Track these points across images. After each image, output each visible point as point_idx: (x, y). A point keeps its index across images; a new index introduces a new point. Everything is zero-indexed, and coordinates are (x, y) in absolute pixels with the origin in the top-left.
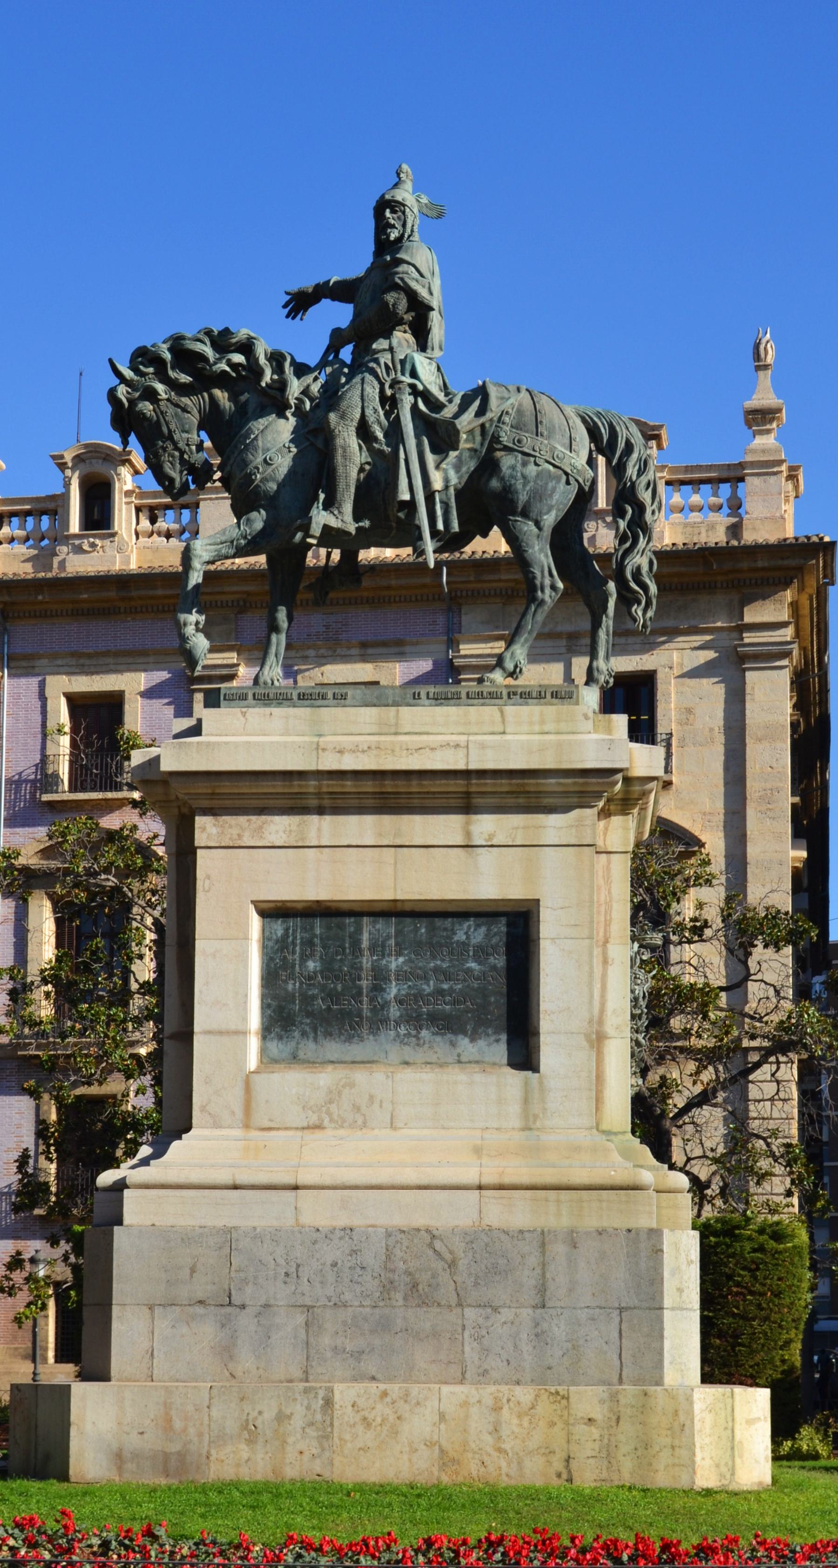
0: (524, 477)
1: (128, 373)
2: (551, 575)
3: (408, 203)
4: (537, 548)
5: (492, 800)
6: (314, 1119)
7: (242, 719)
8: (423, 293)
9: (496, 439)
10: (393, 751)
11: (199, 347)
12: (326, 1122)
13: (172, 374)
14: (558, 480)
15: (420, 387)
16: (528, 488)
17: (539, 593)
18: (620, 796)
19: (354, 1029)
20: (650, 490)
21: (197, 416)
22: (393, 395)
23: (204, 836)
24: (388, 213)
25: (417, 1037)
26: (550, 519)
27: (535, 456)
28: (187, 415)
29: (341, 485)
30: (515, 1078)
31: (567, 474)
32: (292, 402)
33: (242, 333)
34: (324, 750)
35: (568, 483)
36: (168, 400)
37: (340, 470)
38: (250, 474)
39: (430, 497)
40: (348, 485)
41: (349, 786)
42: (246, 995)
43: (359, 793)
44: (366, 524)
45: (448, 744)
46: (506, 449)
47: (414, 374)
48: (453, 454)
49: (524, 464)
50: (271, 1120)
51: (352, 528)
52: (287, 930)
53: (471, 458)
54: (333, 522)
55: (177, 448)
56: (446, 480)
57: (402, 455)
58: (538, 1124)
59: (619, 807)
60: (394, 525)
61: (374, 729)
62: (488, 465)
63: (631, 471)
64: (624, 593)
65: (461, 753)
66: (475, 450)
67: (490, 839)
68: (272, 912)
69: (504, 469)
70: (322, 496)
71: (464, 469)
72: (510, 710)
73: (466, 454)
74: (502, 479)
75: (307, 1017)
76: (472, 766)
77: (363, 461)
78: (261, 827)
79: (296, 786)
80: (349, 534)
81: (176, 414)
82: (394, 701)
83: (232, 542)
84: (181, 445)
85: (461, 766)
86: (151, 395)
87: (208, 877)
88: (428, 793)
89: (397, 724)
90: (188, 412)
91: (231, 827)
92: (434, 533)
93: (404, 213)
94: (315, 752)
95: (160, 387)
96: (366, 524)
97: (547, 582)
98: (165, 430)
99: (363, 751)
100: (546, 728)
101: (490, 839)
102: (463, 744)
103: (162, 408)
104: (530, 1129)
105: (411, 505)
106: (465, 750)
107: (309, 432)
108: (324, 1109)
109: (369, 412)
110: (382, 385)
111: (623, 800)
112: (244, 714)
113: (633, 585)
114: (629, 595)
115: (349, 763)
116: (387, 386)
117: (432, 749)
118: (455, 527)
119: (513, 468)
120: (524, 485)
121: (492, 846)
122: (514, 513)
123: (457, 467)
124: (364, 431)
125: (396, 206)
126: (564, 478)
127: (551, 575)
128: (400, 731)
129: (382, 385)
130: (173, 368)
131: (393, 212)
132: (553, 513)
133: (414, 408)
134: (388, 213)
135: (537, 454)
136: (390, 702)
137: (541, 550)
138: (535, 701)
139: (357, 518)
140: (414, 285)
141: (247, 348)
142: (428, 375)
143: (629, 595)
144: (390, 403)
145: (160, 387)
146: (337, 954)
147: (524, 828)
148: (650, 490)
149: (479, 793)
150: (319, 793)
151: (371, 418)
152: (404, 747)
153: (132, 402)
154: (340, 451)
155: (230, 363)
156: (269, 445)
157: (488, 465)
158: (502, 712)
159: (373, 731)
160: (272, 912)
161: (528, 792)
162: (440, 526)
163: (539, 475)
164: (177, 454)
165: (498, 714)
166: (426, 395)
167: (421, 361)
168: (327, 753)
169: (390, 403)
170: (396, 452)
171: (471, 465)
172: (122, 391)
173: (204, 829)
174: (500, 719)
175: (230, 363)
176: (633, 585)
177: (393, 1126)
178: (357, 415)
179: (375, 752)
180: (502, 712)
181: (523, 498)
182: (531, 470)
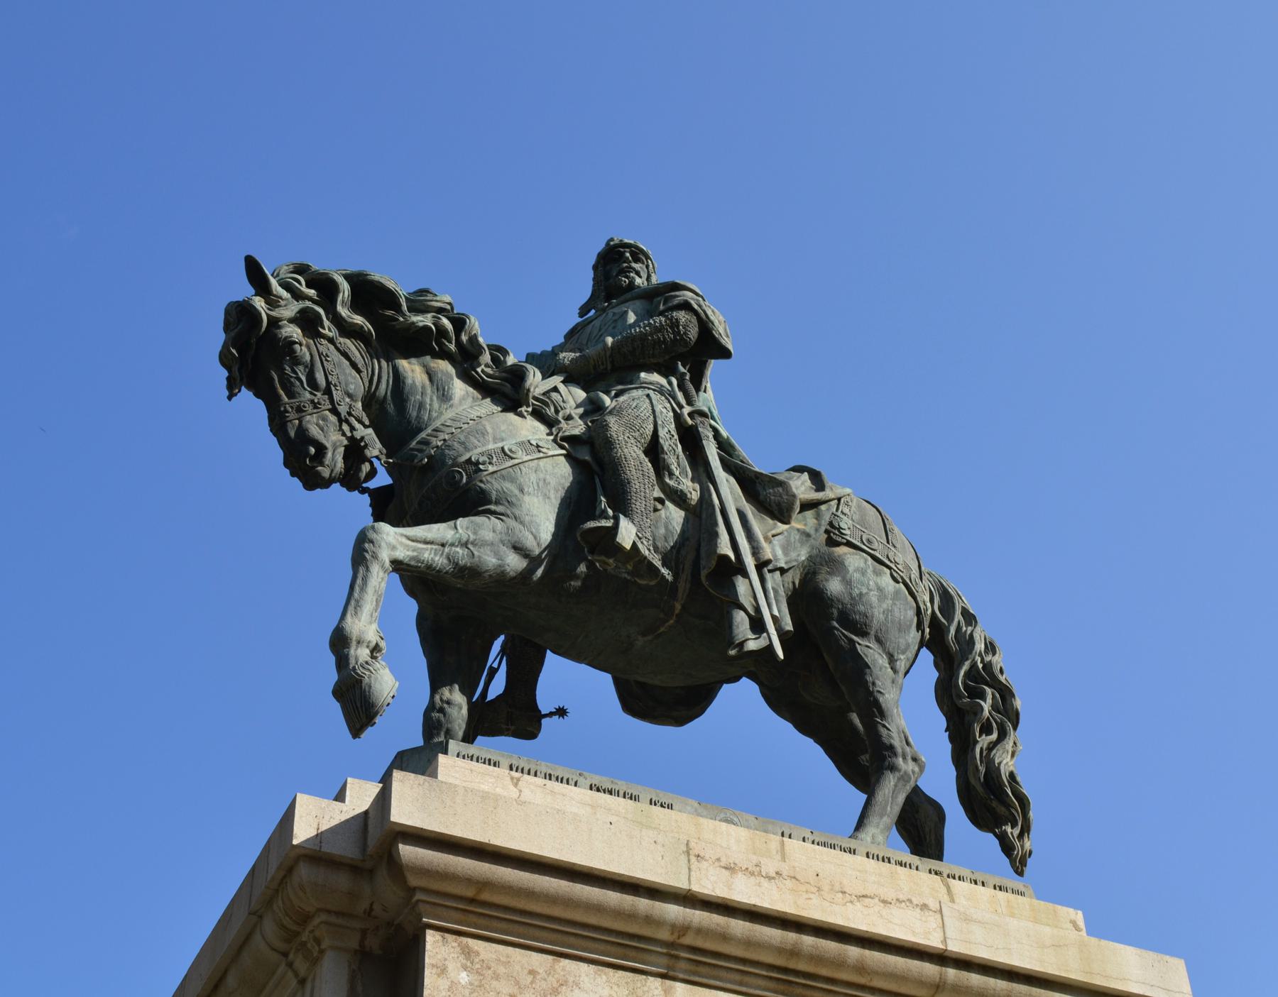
13: (344, 311)
16: (885, 606)
21: (367, 385)
27: (890, 568)
28: (354, 373)
38: (478, 463)
43: (744, 961)
45: (910, 901)
48: (782, 527)
55: (334, 411)
60: (678, 607)
64: (994, 804)
66: (808, 535)
69: (851, 569)
73: (796, 537)
74: (848, 583)
76: (956, 947)
81: (340, 365)
83: (443, 545)
90: (359, 371)
91: (497, 977)
94: (684, 858)
98: (320, 377)
99: (770, 878)
103: (321, 348)
109: (662, 433)
115: (744, 892)
117: (884, 902)
122: (864, 634)
135: (892, 565)
143: (1001, 810)
150: (671, 945)
152: (837, 888)
164: (333, 418)
168: (704, 864)
173: (443, 971)
179: (789, 883)
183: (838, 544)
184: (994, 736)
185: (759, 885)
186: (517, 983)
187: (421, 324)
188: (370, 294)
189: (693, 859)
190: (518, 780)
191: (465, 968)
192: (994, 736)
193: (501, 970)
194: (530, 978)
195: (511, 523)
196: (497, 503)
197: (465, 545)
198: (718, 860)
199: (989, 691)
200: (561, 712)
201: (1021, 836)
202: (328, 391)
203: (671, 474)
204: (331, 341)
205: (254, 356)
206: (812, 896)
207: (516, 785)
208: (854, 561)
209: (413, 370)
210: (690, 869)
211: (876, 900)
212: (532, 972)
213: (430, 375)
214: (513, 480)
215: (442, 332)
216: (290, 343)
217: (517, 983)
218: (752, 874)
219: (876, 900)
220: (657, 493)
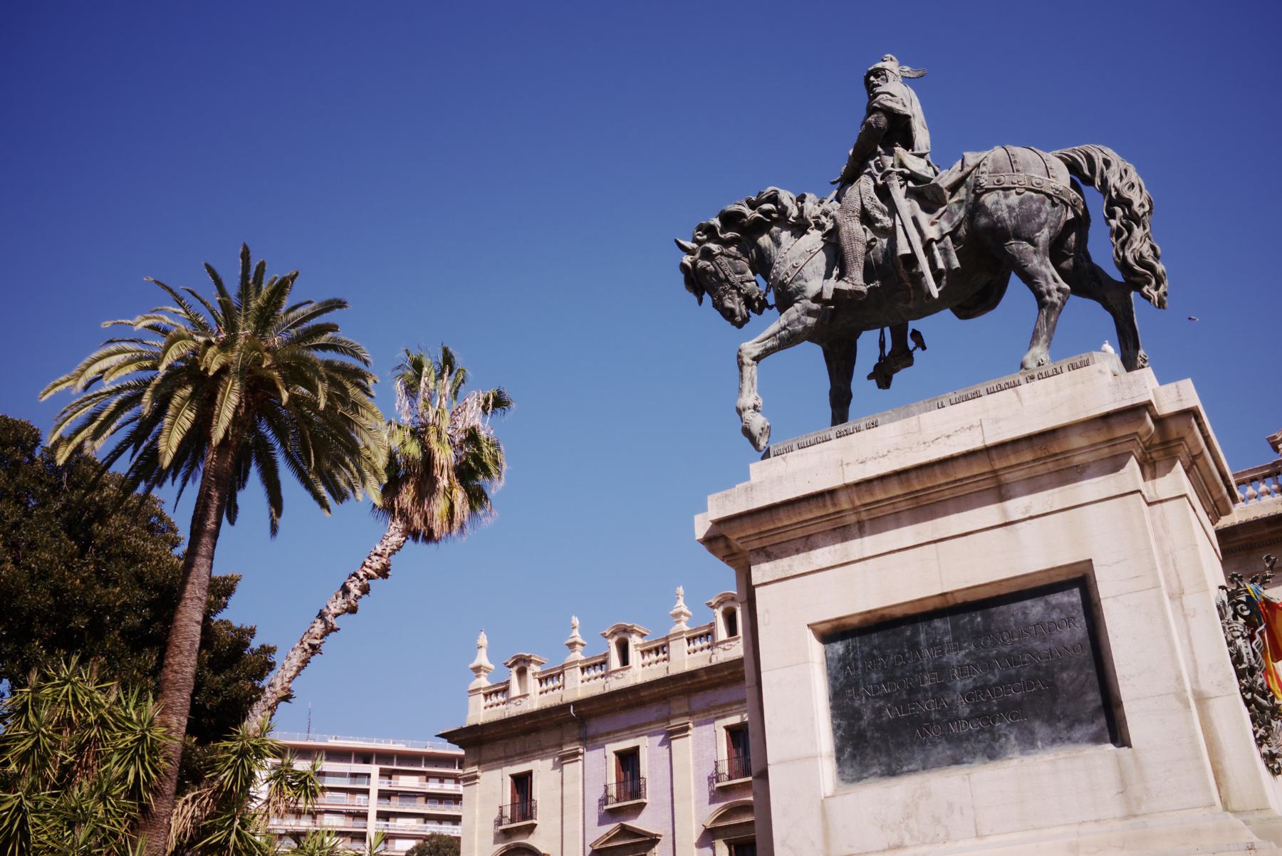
0: (1009, 207)
1: (689, 244)
2: (1056, 281)
4: (1036, 262)
5: (1022, 473)
6: (894, 839)
8: (898, 107)
9: (977, 185)
11: (734, 208)
12: (907, 841)
14: (1044, 203)
15: (907, 171)
17: (1047, 298)
19: (926, 735)
20: (1137, 188)
22: (885, 184)
23: (760, 573)
24: (872, 78)
25: (991, 732)
26: (1044, 236)
29: (850, 258)
30: (1101, 757)
31: (1049, 196)
32: (811, 221)
33: (769, 189)
35: (1054, 205)
36: (721, 254)
37: (847, 248)
40: (855, 258)
42: (813, 718)
44: (878, 283)
46: (988, 190)
47: (902, 165)
49: (1006, 197)
50: (851, 846)
51: (864, 289)
52: (847, 647)
53: (960, 208)
54: (843, 285)
57: (898, 222)
58: (1144, 809)
59: (1161, 453)
62: (976, 208)
63: (1113, 180)
67: (1027, 511)
68: (831, 634)
70: (835, 272)
72: (1025, 388)
75: (877, 731)
80: (861, 293)
84: (737, 283)
85: (978, 444)
86: (708, 255)
87: (767, 611)
88: (955, 481)
92: (937, 275)
95: (714, 247)
96: (878, 283)
97: (1053, 286)
98: (722, 276)
101: (1027, 511)
102: (976, 423)
104: (1136, 816)
105: (911, 259)
108: (903, 826)
110: (875, 180)
111: (1162, 444)
112: (784, 459)
113: (1137, 268)
114: (1138, 279)
116: (878, 179)
118: (956, 263)
119: (997, 203)
120: (1010, 213)
121: (1031, 518)
123: (950, 220)
124: (866, 218)
125: (878, 73)
126: (1048, 201)
127: (1056, 281)
129: (875, 180)
130: (722, 232)
131: (877, 76)
132: (1046, 231)
134: (872, 78)
137: (1042, 263)
139: (867, 280)
140: (889, 104)
141: (774, 199)
142: (917, 165)
143: (1138, 279)
144: (883, 192)
145: (714, 247)
146: (898, 660)
149: (1005, 468)
151: (869, 207)
153: (694, 263)
154: (845, 235)
155: (762, 212)
157: (976, 208)
158: (1017, 393)
160: (831, 634)
161: (1056, 455)
162: (941, 265)
163: (1021, 203)
166: (914, 177)
169: (883, 192)
170: (894, 224)
171: (962, 213)
172: (687, 260)
175: (762, 212)
176: (1137, 268)
177: (978, 836)
178: (858, 206)
180: (1017, 393)
181: (1010, 223)
182: (1014, 199)
183: (982, 194)
184: (1126, 234)
188: (730, 219)
192: (1126, 234)
195: (803, 302)
196: (797, 294)
197: (784, 328)
199: (1118, 209)
201: (1157, 288)
202: (727, 280)
203: (877, 220)
204: (721, 254)
205: (698, 282)
208: (989, 200)
209: (764, 240)
213: (771, 236)
214: (801, 278)
215: (767, 213)
216: (704, 269)
220: (870, 236)
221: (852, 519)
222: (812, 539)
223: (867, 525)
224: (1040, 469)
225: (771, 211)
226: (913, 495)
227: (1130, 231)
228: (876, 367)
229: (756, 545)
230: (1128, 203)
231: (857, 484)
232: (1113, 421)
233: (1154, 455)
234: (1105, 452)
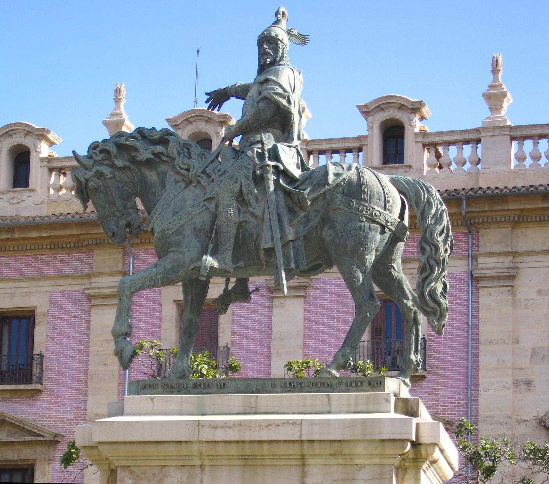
3: (280, 37)
7: (151, 404)
10: (250, 427)
15: (282, 168)
18: (411, 456)
20: (444, 235)
22: (262, 175)
31: (383, 226)
34: (203, 426)
39: (285, 245)
41: (221, 450)
56: (297, 232)
59: (412, 464)
61: (241, 410)
64: (425, 308)
65: (297, 428)
70: (211, 247)
71: (310, 225)
77: (241, 220)
78: (162, 480)
79: (184, 450)
82: (257, 389)
85: (297, 438)
89: (256, 407)
91: (141, 479)
93: (277, 44)
94: (197, 428)
99: (230, 427)
100: (359, 409)
106: (300, 426)
107: (205, 200)
117: (278, 426)
128: (258, 411)
132: (374, 253)
133: (276, 182)
136: (254, 389)
138: (354, 389)
147: (342, 480)
148: (444, 235)
152: (258, 424)
156: (178, 210)
159: (240, 411)
165: (326, 399)
167: (282, 148)
168: (205, 428)
174: (327, 403)
179: (238, 428)
180: (328, 396)
184: (428, 272)
185: (226, 431)
186: (148, 480)
187: (145, 158)
189: (200, 427)
190: (153, 399)
191: (130, 478)
193: (143, 476)
194: (152, 477)
198: (210, 425)
200: (257, 289)
206: (247, 431)
207: (152, 401)
210: (199, 432)
211: (274, 426)
212: (154, 475)
213: (158, 174)
217: (148, 480)
218: (223, 427)
219: (274, 426)
221: (198, 462)
222: (165, 469)
223: (207, 469)
224: (333, 461)
225: (162, 153)
226: (245, 457)
227: (432, 270)
228: (220, 296)
229: (124, 463)
230: (437, 248)
231: (208, 442)
232: (386, 444)
233: (407, 464)
234: (377, 461)
